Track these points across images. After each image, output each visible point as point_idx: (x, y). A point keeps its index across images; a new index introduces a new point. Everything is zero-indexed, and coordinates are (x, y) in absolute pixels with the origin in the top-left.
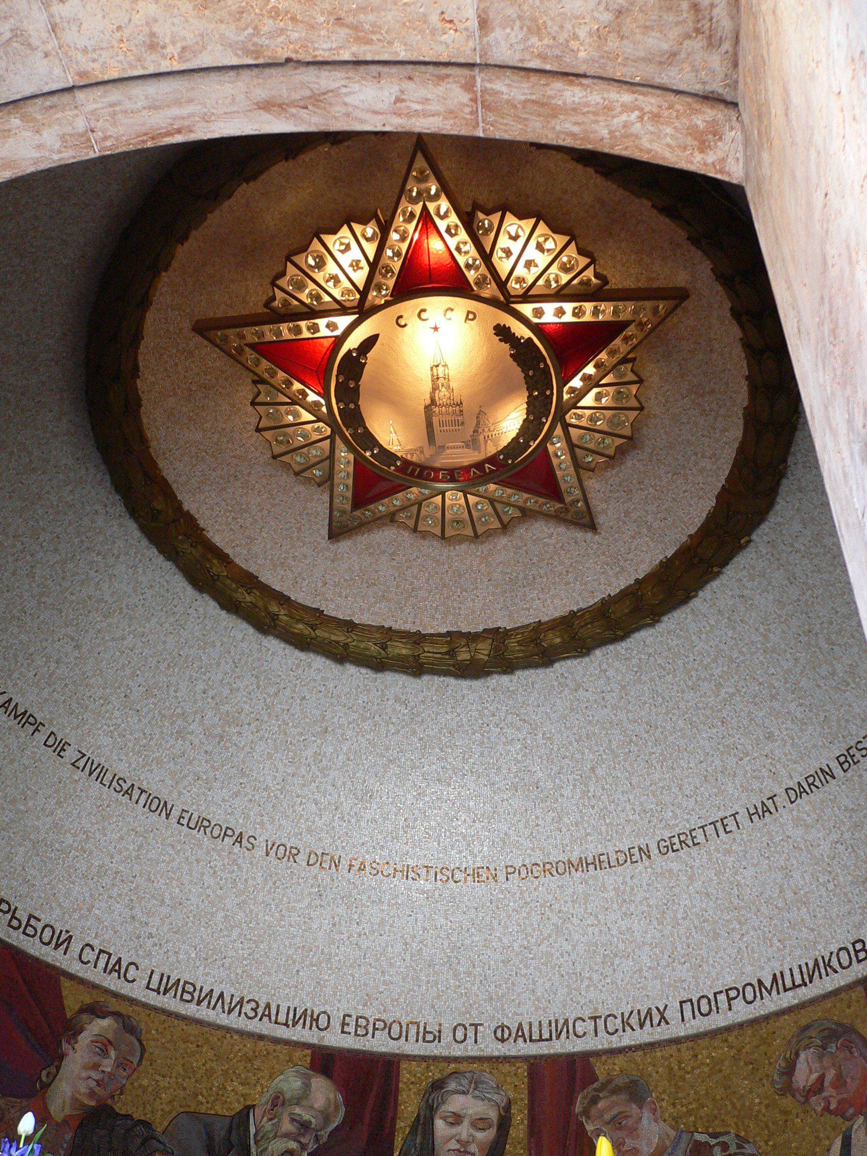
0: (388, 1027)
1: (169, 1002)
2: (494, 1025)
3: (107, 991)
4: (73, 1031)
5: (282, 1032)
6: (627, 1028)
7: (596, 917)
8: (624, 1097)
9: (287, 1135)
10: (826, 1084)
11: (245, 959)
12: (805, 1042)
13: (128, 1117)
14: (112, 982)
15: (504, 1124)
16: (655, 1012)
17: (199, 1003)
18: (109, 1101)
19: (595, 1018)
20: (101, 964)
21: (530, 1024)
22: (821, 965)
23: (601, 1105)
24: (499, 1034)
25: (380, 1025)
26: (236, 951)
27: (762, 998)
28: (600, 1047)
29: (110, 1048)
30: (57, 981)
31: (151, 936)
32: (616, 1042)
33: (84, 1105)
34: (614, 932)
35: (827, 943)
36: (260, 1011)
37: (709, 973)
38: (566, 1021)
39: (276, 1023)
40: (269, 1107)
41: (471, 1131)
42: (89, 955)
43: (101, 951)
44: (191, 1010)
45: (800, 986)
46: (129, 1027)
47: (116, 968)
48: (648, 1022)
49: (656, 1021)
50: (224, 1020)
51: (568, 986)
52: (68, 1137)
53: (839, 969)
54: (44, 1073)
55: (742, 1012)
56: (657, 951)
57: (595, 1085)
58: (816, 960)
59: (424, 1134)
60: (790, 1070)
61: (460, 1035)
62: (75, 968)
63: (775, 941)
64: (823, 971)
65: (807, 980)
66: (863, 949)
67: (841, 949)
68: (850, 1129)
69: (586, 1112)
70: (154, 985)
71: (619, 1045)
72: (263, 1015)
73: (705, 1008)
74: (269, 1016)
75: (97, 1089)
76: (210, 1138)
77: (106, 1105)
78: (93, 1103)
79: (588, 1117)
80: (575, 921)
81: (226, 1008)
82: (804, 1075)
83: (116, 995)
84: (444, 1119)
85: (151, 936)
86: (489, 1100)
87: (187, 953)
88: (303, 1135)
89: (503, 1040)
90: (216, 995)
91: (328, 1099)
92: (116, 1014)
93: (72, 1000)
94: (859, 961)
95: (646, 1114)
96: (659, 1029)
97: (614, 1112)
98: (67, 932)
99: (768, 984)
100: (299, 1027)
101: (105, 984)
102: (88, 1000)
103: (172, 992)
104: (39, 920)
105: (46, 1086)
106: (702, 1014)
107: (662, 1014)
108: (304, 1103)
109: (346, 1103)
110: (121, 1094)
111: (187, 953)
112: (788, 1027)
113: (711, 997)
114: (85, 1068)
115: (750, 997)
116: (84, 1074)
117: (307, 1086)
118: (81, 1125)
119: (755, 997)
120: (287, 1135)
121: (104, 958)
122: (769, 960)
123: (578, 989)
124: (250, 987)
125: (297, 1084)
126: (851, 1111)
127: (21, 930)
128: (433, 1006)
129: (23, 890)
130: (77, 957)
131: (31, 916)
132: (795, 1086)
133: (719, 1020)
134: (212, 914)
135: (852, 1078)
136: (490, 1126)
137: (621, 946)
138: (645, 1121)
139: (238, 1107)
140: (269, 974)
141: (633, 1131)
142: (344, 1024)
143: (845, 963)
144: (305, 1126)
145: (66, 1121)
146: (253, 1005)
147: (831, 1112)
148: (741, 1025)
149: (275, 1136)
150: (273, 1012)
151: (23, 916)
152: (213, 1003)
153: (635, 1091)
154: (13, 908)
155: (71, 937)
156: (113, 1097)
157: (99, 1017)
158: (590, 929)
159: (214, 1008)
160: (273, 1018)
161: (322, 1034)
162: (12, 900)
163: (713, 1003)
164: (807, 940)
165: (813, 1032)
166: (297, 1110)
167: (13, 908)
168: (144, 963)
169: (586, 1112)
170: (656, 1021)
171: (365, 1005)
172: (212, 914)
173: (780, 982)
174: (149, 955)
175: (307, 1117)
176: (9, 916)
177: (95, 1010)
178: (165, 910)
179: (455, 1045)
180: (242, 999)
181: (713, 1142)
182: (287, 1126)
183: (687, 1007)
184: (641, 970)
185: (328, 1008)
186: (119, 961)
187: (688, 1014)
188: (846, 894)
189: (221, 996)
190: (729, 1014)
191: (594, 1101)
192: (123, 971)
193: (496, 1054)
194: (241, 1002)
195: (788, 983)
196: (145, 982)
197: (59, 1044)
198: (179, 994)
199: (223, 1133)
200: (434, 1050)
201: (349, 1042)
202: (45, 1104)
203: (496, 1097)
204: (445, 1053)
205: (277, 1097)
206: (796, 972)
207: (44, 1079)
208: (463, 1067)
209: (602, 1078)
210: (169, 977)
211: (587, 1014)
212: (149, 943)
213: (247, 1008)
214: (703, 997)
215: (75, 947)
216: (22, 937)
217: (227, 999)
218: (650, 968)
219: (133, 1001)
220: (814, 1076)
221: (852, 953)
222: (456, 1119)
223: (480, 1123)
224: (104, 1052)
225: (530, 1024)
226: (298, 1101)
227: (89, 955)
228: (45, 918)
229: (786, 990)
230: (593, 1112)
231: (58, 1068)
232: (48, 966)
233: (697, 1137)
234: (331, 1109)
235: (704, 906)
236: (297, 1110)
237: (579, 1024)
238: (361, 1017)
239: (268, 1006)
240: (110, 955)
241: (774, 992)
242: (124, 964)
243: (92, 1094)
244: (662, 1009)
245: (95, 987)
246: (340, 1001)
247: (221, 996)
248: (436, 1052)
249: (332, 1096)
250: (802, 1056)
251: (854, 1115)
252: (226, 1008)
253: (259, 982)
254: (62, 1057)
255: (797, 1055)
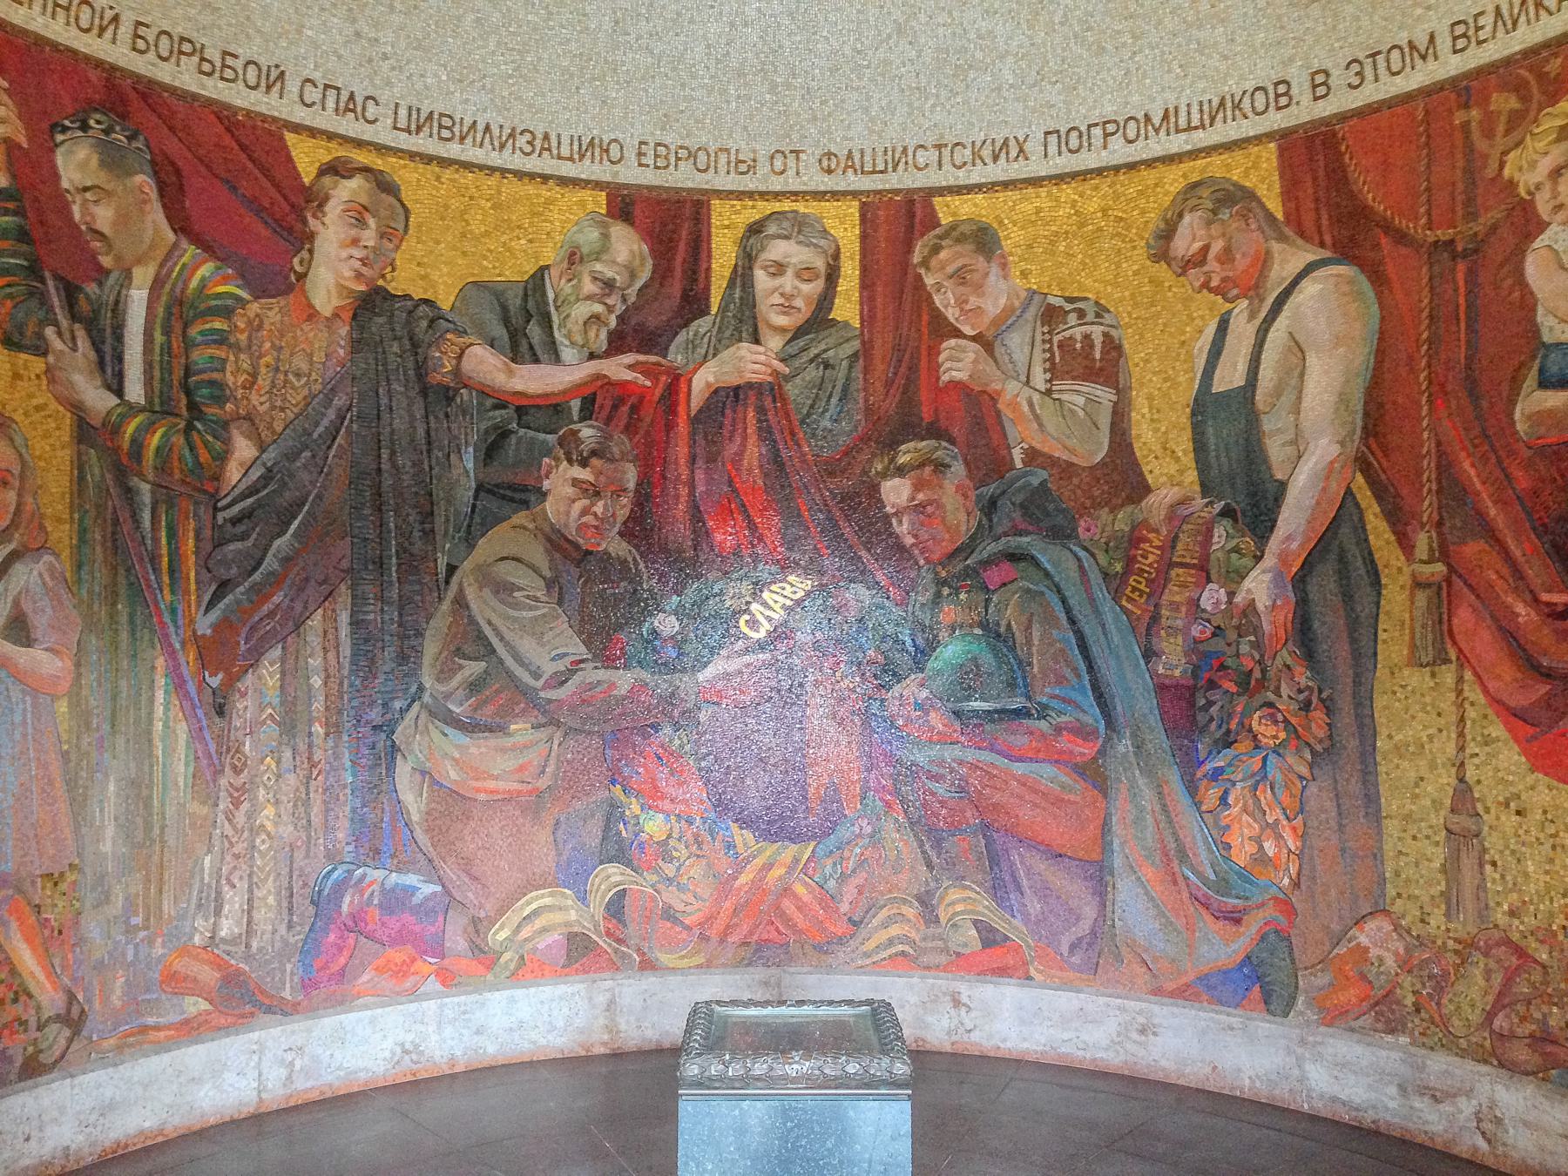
0: (692, 155)
1: (424, 143)
2: (819, 152)
3: (346, 140)
4: (313, 199)
5: (568, 170)
6: (978, 161)
7: (950, 13)
8: (970, 247)
9: (589, 298)
10: (1211, 255)
11: (510, 77)
12: (1194, 202)
13: (407, 297)
14: (349, 126)
15: (832, 276)
16: (1012, 143)
17: (462, 139)
18: (380, 282)
19: (939, 147)
20: (331, 104)
21: (862, 152)
22: (1229, 105)
23: (943, 255)
24: (825, 163)
25: (683, 153)
26: (498, 67)
27: (1146, 138)
28: (944, 184)
29: (367, 215)
30: (282, 139)
31: (385, 57)
32: (962, 177)
33: (352, 291)
34: (973, 36)
35: (1242, 78)
36: (538, 143)
37: (1085, 99)
38: (905, 149)
39: (560, 158)
40: (565, 265)
41: (797, 283)
42: (313, 94)
43: (327, 86)
44: (453, 150)
45: (1196, 128)
46: (385, 185)
47: (349, 106)
48: (1003, 155)
49: (1013, 153)
50: (495, 159)
51: (910, 105)
52: (344, 331)
53: (1250, 114)
54: (296, 261)
55: (1119, 152)
56: (1023, 64)
57: (937, 231)
58: (1223, 98)
59: (743, 286)
60: (1167, 233)
61: (778, 164)
62: (300, 115)
63: (1175, 65)
64: (1229, 113)
65: (1207, 122)
66: (1286, 94)
67: (1258, 89)
68: (1230, 312)
69: (925, 263)
70: (402, 123)
71: (967, 182)
72: (543, 149)
73: (1074, 143)
74: (549, 150)
75: (364, 270)
76: (504, 308)
77: (381, 287)
78: (362, 288)
79: (928, 269)
80: (923, 18)
81: (496, 143)
82: (1185, 243)
83: (359, 144)
84: (765, 268)
85: (385, 57)
86: (816, 246)
87: (436, 75)
88: (609, 295)
89: (829, 171)
90: (480, 127)
91: (631, 251)
92: (366, 170)
93: (307, 158)
94: (1279, 109)
95: (995, 269)
96: (1016, 165)
97: (959, 263)
98: (277, 66)
99: (1157, 121)
100: (587, 161)
101: (341, 131)
102: (328, 158)
103: (426, 129)
104: (236, 57)
105: (302, 277)
106: (1070, 151)
107: (1021, 151)
108: (605, 257)
109: (652, 250)
110: (393, 270)
111: (436, 75)
112: (1174, 180)
113: (1083, 129)
114: (343, 246)
115: (1131, 134)
116: (344, 254)
117: (606, 236)
118: (355, 317)
119: (1138, 136)
120: (589, 298)
121: (331, 96)
122: (1163, 90)
123: (921, 109)
124: (521, 113)
125: (594, 234)
126: (1235, 292)
127: (217, 75)
128: (745, 128)
129: (205, 19)
130: (297, 99)
131: (225, 53)
132: (1172, 254)
133: (1089, 160)
134: (459, 18)
135: (1244, 255)
136: (817, 277)
137: (979, 55)
138: (992, 278)
139: (531, 269)
140: (543, 95)
141: (979, 288)
142: (640, 154)
143: (1260, 108)
144: (609, 285)
145: (336, 315)
146: (528, 137)
147: (1210, 290)
148: (1116, 169)
149: (578, 300)
150: (554, 144)
151: (213, 54)
152: (479, 140)
153: (983, 240)
154: (198, 46)
155: (283, 73)
156: (383, 276)
157: (344, 177)
158: (941, 30)
159: (481, 145)
160: (555, 152)
161: (616, 168)
162: (194, 35)
163: (1085, 138)
164: (1217, 69)
165: (1205, 192)
166: (598, 267)
167: (198, 46)
168: (384, 96)
169: (925, 263)
170: (1013, 153)
171: (663, 129)
172: (459, 18)
173: (1173, 120)
174: (389, 83)
175: (610, 274)
176: (196, 59)
177: (335, 169)
178: (397, 19)
179: (774, 178)
180: (513, 129)
181: (1068, 307)
182: (589, 287)
183: (1053, 139)
184: (999, 89)
185: (620, 136)
186: (352, 97)
187: (1052, 149)
188: (1279, 18)
189: (487, 128)
190: (1104, 153)
191: (936, 249)
192: (359, 109)
193: (822, 188)
194: (512, 135)
195: (1182, 122)
196: (389, 121)
197: (305, 222)
198: (435, 131)
199: (518, 302)
200: (749, 183)
201: (648, 177)
202: (307, 298)
203: (822, 242)
204: (762, 188)
205: (573, 254)
206: (1195, 109)
207: (298, 268)
208: (786, 205)
209: (945, 219)
210: (418, 110)
211: (930, 140)
212: (386, 65)
213: (522, 141)
214: (1073, 129)
215: (293, 86)
216: (221, 84)
217: (496, 132)
218: (1011, 86)
219: (381, 149)
220: (1197, 245)
221: (1272, 96)
222: (779, 269)
223: (806, 273)
224: (361, 223)
225: (862, 152)
226: (597, 256)
227: (313, 94)
228: (244, 52)
229: (1178, 131)
230: (934, 263)
231: (311, 251)
232: (264, 118)
233: (1051, 300)
234: (637, 262)
235: (1090, 8)
236: (598, 267)
237: (920, 152)
238: (659, 144)
239: (546, 137)
240: (338, 89)
241: (1163, 132)
242: (359, 100)
243: (359, 276)
244: (1021, 140)
245: (330, 136)
246: (633, 126)
247: (487, 128)
248: (751, 187)
249: (635, 247)
250: (1187, 219)
251: (1237, 297)
252: (496, 143)
253: (531, 106)
254: (311, 237)
255: (1181, 215)
